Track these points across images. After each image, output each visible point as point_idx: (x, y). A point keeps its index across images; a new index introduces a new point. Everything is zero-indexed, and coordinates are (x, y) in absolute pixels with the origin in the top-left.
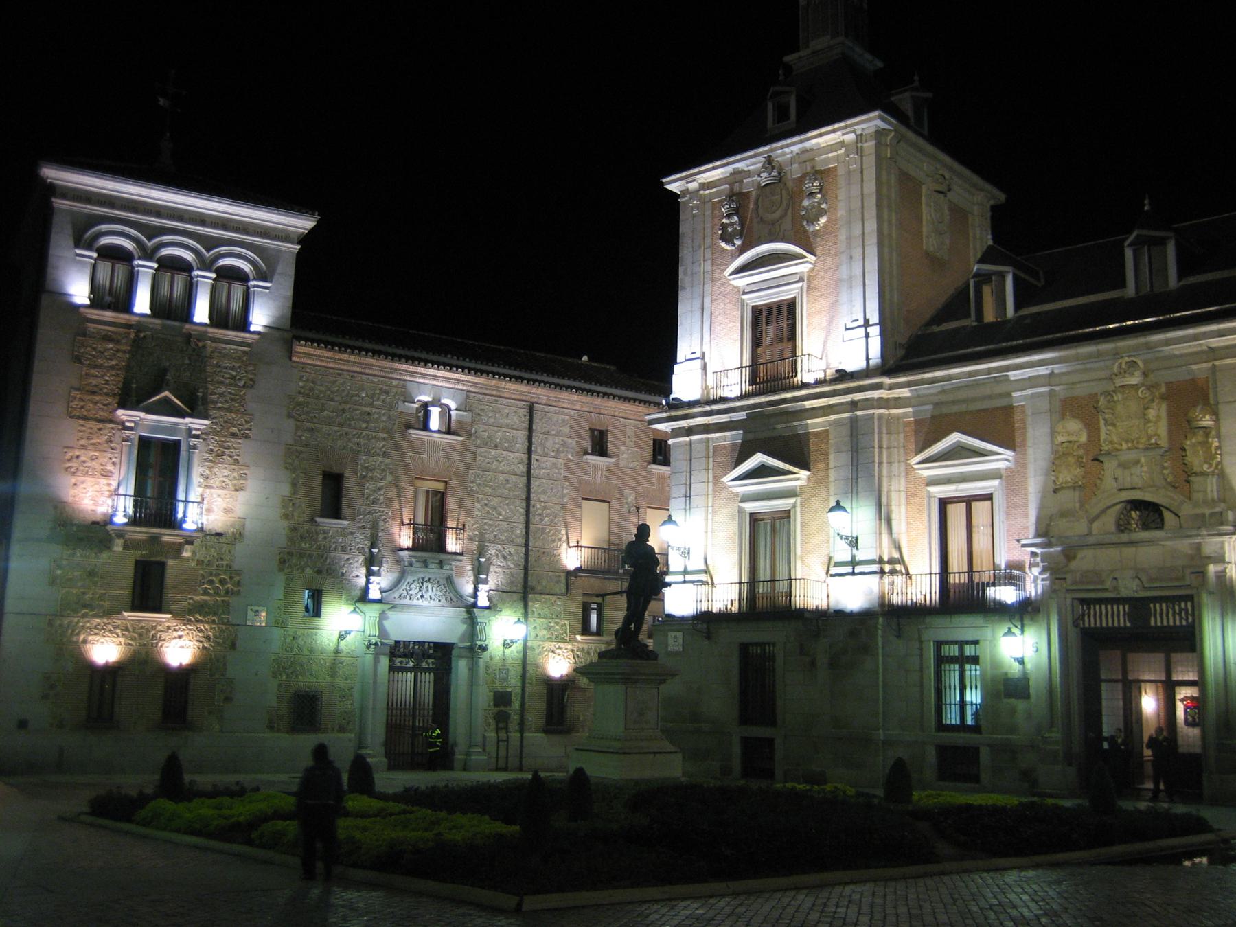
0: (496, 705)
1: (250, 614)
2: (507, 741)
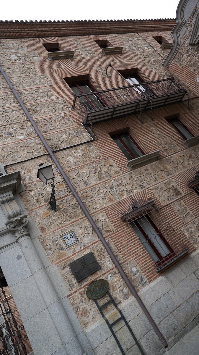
0: (80, 279)
2: (123, 318)
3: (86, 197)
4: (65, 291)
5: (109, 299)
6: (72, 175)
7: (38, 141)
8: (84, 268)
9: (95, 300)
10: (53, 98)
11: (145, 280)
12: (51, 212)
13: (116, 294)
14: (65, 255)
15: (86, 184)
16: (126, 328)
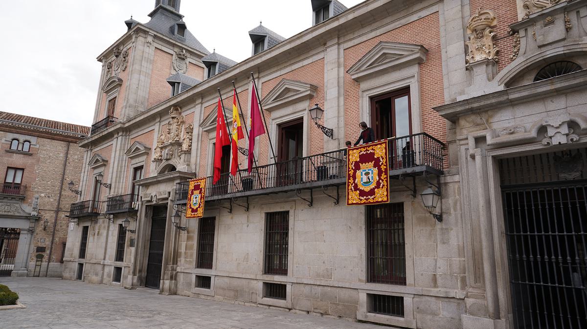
0: (37, 251)
3: (57, 231)
4: (31, 251)
6: (59, 222)
7: (57, 204)
8: (41, 250)
12: (43, 230)
13: (44, 260)
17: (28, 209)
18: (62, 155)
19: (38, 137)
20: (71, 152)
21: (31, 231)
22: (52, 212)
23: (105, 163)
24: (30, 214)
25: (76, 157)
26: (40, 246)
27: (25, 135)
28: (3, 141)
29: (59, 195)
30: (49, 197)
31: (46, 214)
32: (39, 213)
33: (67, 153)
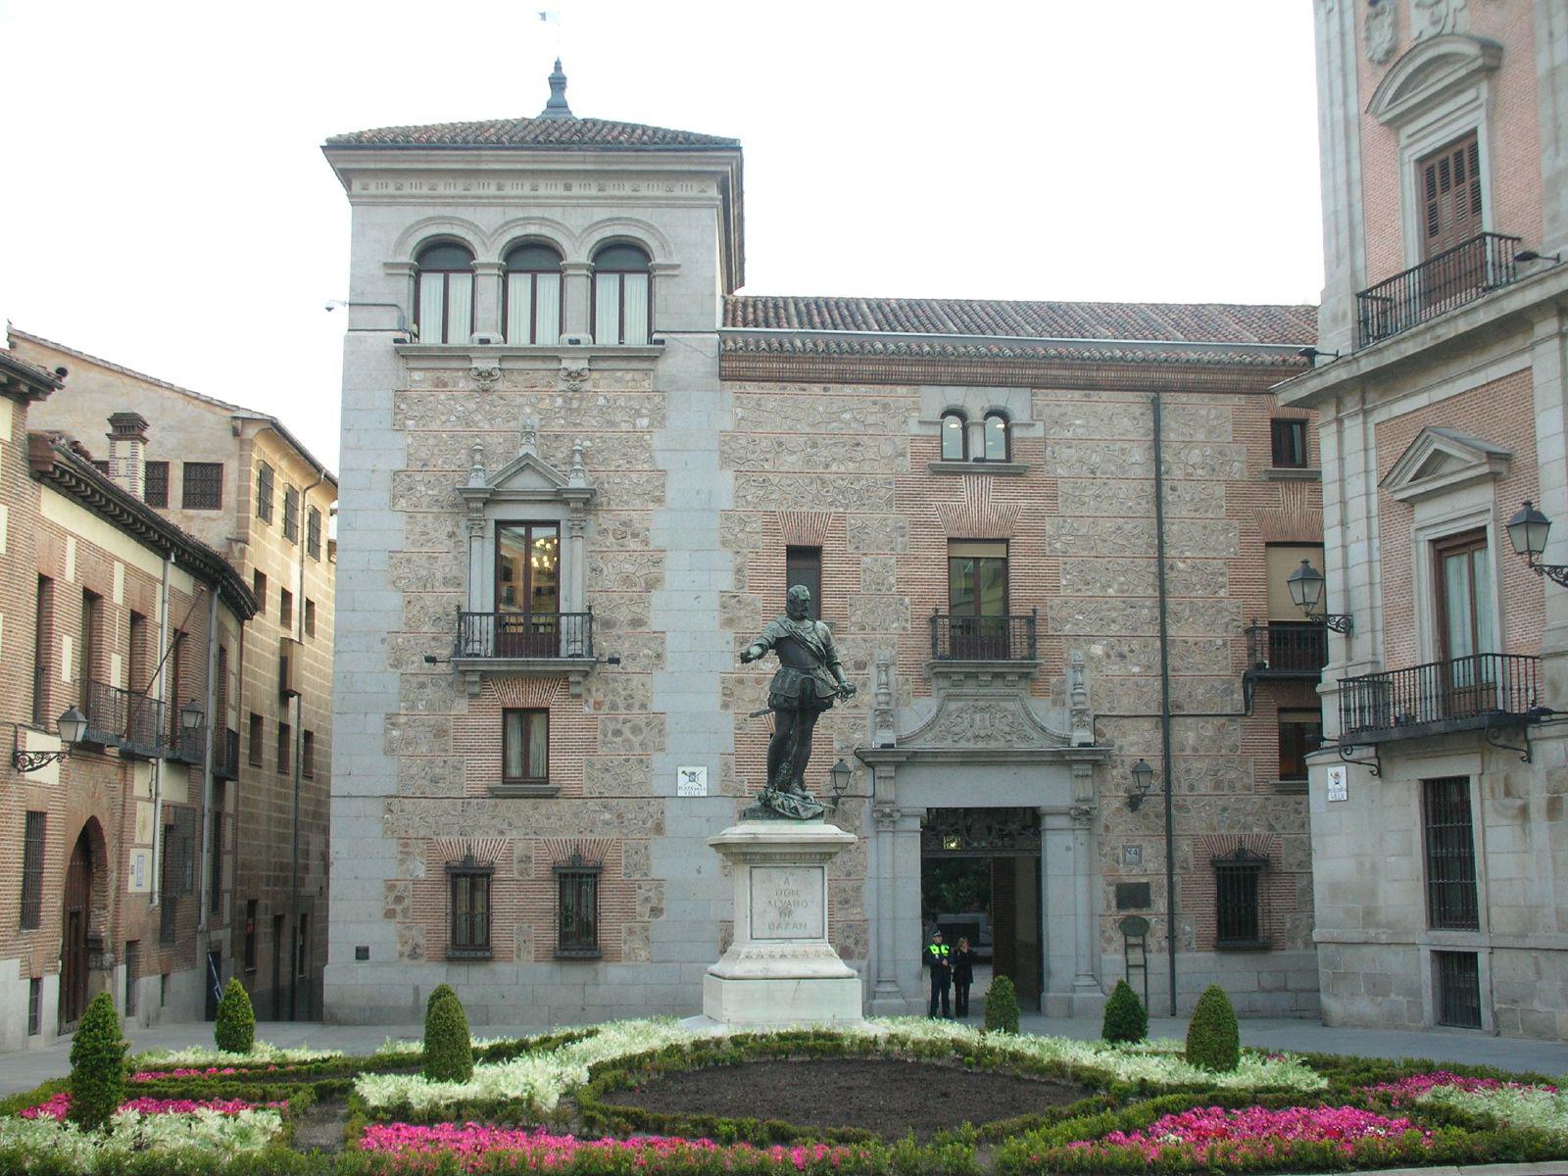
0: (1121, 905)
1: (682, 780)
2: (1145, 967)
3: (1180, 808)
5: (1141, 942)
6: (1179, 767)
8: (1131, 896)
9: (1126, 935)
10: (1222, 593)
11: (1194, 945)
12: (1126, 810)
13: (1152, 942)
14: (1117, 871)
15: (1191, 788)
16: (1143, 977)
17: (1053, 719)
18: (1138, 456)
19: (1034, 386)
20: (1170, 436)
21: (1084, 815)
22: (1146, 724)
23: (1497, 468)
24: (1067, 741)
25: (1195, 456)
26: (1127, 880)
27: (984, 385)
28: (914, 428)
29: (1158, 644)
30: (1122, 656)
31: (1124, 735)
32: (1095, 732)
33: (1157, 444)
